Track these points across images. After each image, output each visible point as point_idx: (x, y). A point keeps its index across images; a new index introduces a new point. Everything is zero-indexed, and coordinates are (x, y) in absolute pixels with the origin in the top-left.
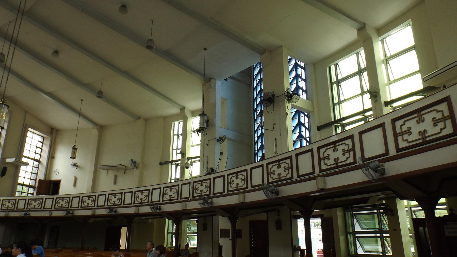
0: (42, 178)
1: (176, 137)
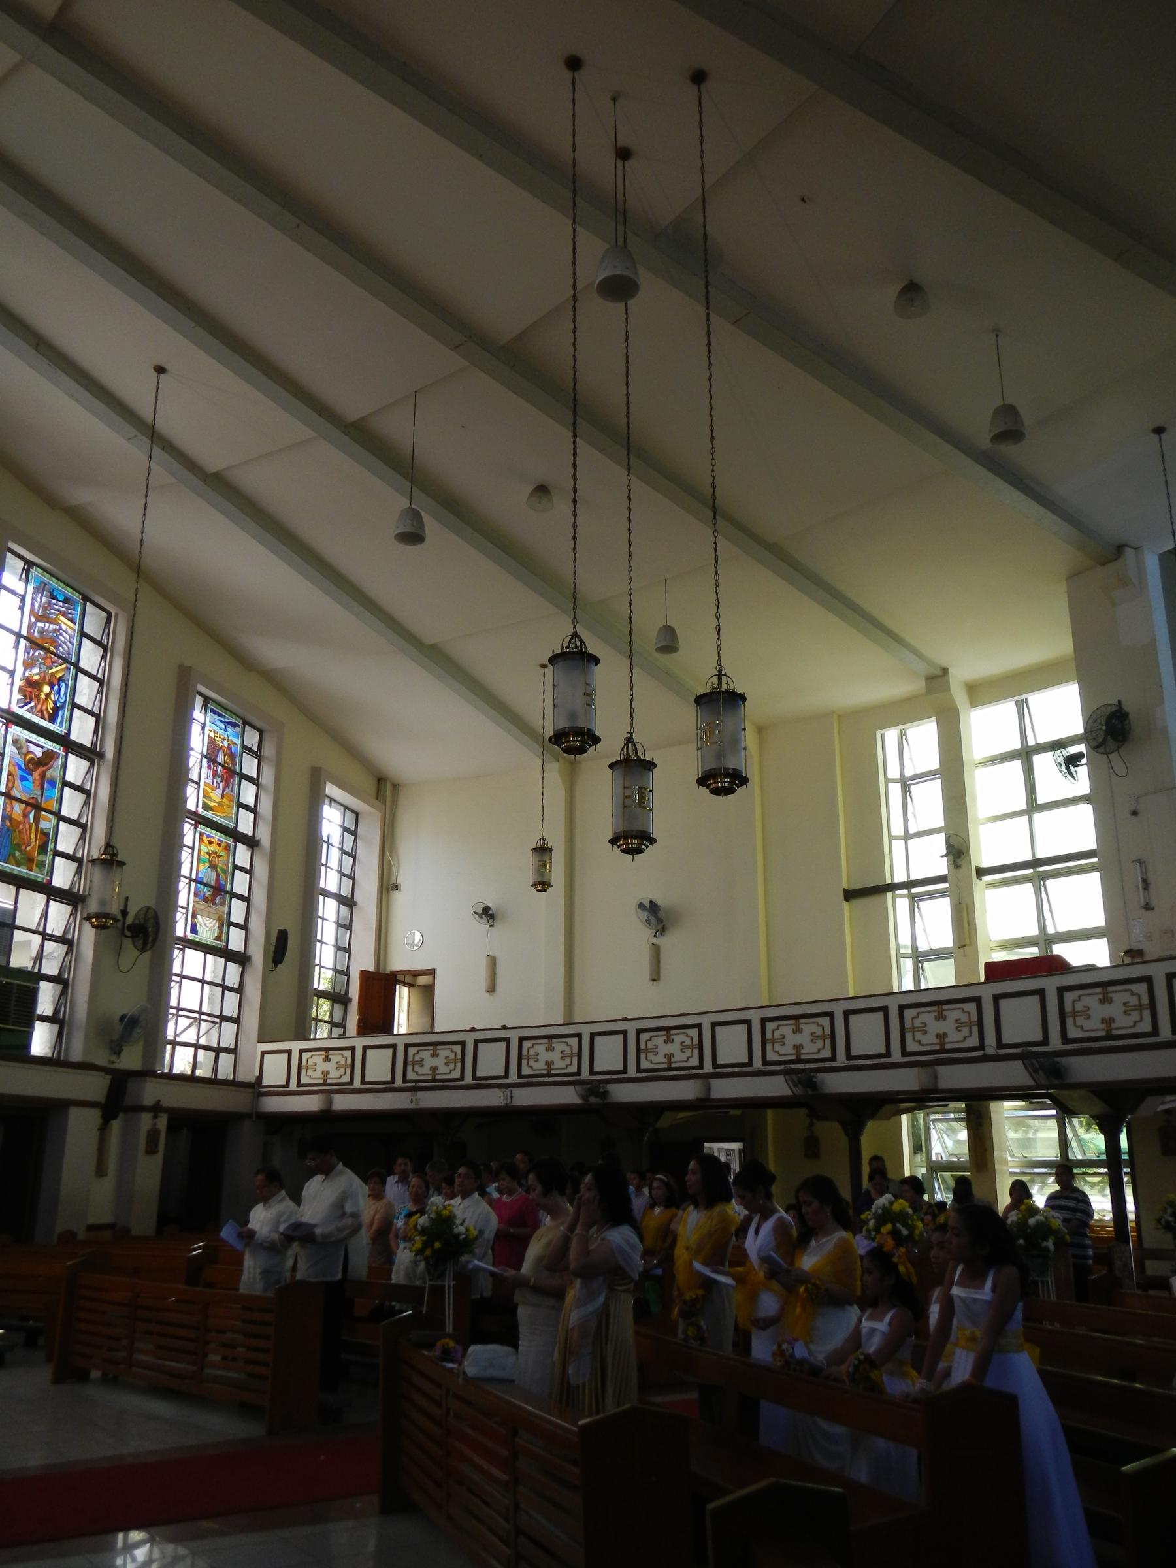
1: (895, 790)
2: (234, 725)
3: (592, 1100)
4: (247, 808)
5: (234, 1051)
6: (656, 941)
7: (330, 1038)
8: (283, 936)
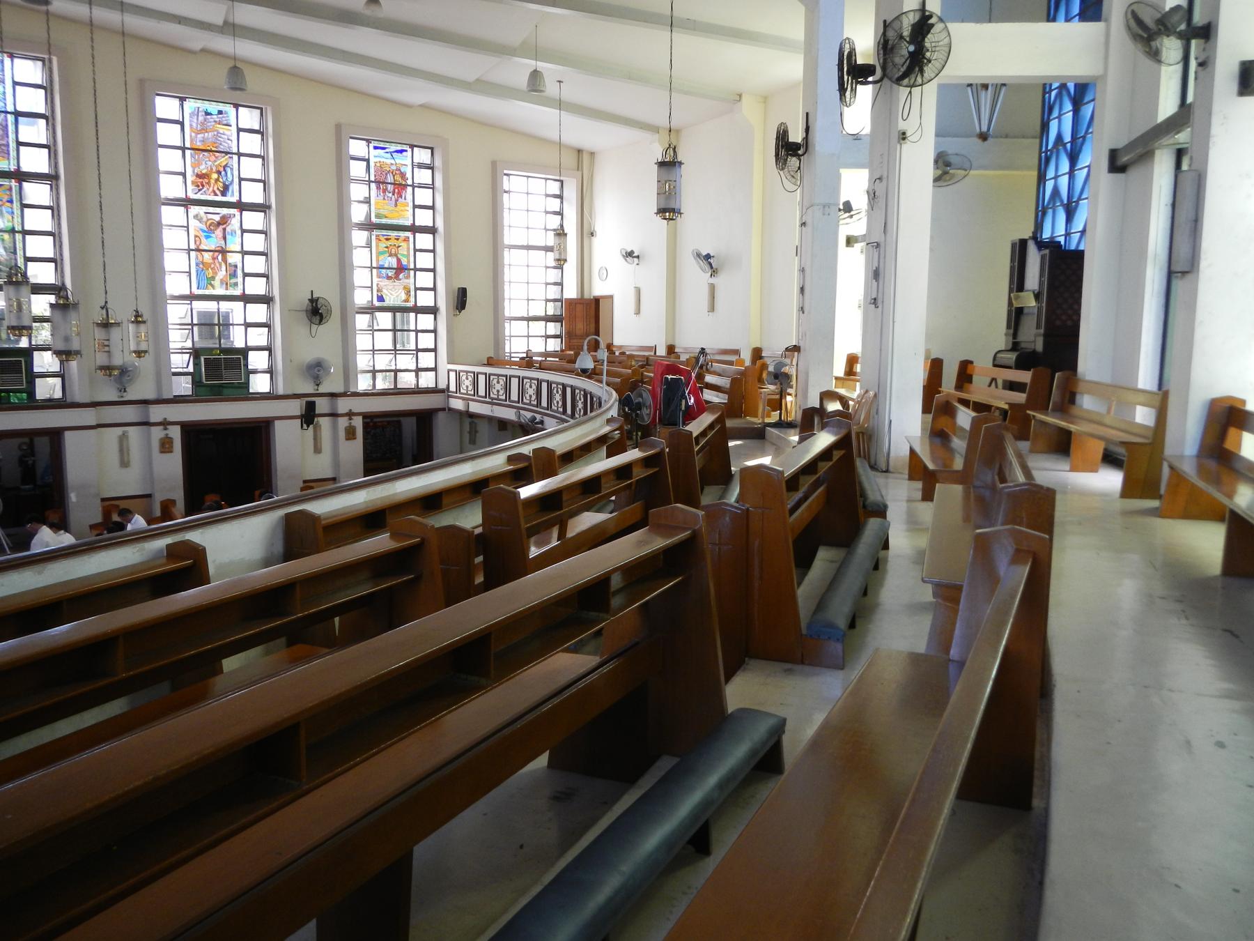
6: (713, 280)
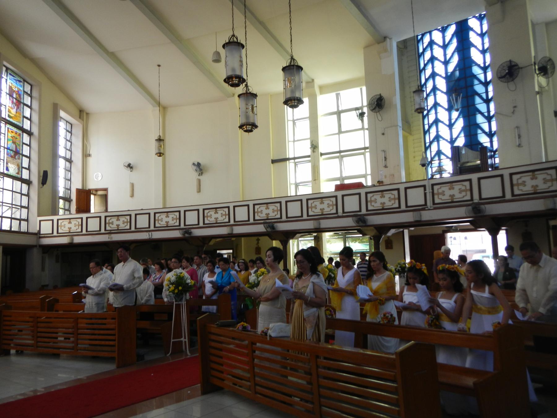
0: (80, 187)
1: (291, 124)
2: (20, 81)
3: (187, 235)
4: (27, 118)
5: (27, 220)
6: (200, 177)
7: (64, 214)
8: (45, 174)
